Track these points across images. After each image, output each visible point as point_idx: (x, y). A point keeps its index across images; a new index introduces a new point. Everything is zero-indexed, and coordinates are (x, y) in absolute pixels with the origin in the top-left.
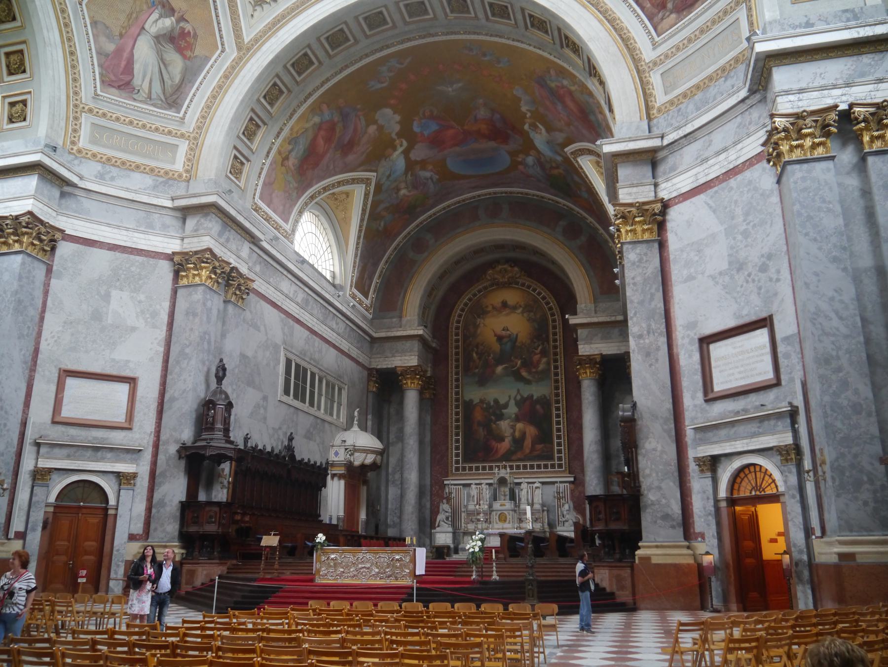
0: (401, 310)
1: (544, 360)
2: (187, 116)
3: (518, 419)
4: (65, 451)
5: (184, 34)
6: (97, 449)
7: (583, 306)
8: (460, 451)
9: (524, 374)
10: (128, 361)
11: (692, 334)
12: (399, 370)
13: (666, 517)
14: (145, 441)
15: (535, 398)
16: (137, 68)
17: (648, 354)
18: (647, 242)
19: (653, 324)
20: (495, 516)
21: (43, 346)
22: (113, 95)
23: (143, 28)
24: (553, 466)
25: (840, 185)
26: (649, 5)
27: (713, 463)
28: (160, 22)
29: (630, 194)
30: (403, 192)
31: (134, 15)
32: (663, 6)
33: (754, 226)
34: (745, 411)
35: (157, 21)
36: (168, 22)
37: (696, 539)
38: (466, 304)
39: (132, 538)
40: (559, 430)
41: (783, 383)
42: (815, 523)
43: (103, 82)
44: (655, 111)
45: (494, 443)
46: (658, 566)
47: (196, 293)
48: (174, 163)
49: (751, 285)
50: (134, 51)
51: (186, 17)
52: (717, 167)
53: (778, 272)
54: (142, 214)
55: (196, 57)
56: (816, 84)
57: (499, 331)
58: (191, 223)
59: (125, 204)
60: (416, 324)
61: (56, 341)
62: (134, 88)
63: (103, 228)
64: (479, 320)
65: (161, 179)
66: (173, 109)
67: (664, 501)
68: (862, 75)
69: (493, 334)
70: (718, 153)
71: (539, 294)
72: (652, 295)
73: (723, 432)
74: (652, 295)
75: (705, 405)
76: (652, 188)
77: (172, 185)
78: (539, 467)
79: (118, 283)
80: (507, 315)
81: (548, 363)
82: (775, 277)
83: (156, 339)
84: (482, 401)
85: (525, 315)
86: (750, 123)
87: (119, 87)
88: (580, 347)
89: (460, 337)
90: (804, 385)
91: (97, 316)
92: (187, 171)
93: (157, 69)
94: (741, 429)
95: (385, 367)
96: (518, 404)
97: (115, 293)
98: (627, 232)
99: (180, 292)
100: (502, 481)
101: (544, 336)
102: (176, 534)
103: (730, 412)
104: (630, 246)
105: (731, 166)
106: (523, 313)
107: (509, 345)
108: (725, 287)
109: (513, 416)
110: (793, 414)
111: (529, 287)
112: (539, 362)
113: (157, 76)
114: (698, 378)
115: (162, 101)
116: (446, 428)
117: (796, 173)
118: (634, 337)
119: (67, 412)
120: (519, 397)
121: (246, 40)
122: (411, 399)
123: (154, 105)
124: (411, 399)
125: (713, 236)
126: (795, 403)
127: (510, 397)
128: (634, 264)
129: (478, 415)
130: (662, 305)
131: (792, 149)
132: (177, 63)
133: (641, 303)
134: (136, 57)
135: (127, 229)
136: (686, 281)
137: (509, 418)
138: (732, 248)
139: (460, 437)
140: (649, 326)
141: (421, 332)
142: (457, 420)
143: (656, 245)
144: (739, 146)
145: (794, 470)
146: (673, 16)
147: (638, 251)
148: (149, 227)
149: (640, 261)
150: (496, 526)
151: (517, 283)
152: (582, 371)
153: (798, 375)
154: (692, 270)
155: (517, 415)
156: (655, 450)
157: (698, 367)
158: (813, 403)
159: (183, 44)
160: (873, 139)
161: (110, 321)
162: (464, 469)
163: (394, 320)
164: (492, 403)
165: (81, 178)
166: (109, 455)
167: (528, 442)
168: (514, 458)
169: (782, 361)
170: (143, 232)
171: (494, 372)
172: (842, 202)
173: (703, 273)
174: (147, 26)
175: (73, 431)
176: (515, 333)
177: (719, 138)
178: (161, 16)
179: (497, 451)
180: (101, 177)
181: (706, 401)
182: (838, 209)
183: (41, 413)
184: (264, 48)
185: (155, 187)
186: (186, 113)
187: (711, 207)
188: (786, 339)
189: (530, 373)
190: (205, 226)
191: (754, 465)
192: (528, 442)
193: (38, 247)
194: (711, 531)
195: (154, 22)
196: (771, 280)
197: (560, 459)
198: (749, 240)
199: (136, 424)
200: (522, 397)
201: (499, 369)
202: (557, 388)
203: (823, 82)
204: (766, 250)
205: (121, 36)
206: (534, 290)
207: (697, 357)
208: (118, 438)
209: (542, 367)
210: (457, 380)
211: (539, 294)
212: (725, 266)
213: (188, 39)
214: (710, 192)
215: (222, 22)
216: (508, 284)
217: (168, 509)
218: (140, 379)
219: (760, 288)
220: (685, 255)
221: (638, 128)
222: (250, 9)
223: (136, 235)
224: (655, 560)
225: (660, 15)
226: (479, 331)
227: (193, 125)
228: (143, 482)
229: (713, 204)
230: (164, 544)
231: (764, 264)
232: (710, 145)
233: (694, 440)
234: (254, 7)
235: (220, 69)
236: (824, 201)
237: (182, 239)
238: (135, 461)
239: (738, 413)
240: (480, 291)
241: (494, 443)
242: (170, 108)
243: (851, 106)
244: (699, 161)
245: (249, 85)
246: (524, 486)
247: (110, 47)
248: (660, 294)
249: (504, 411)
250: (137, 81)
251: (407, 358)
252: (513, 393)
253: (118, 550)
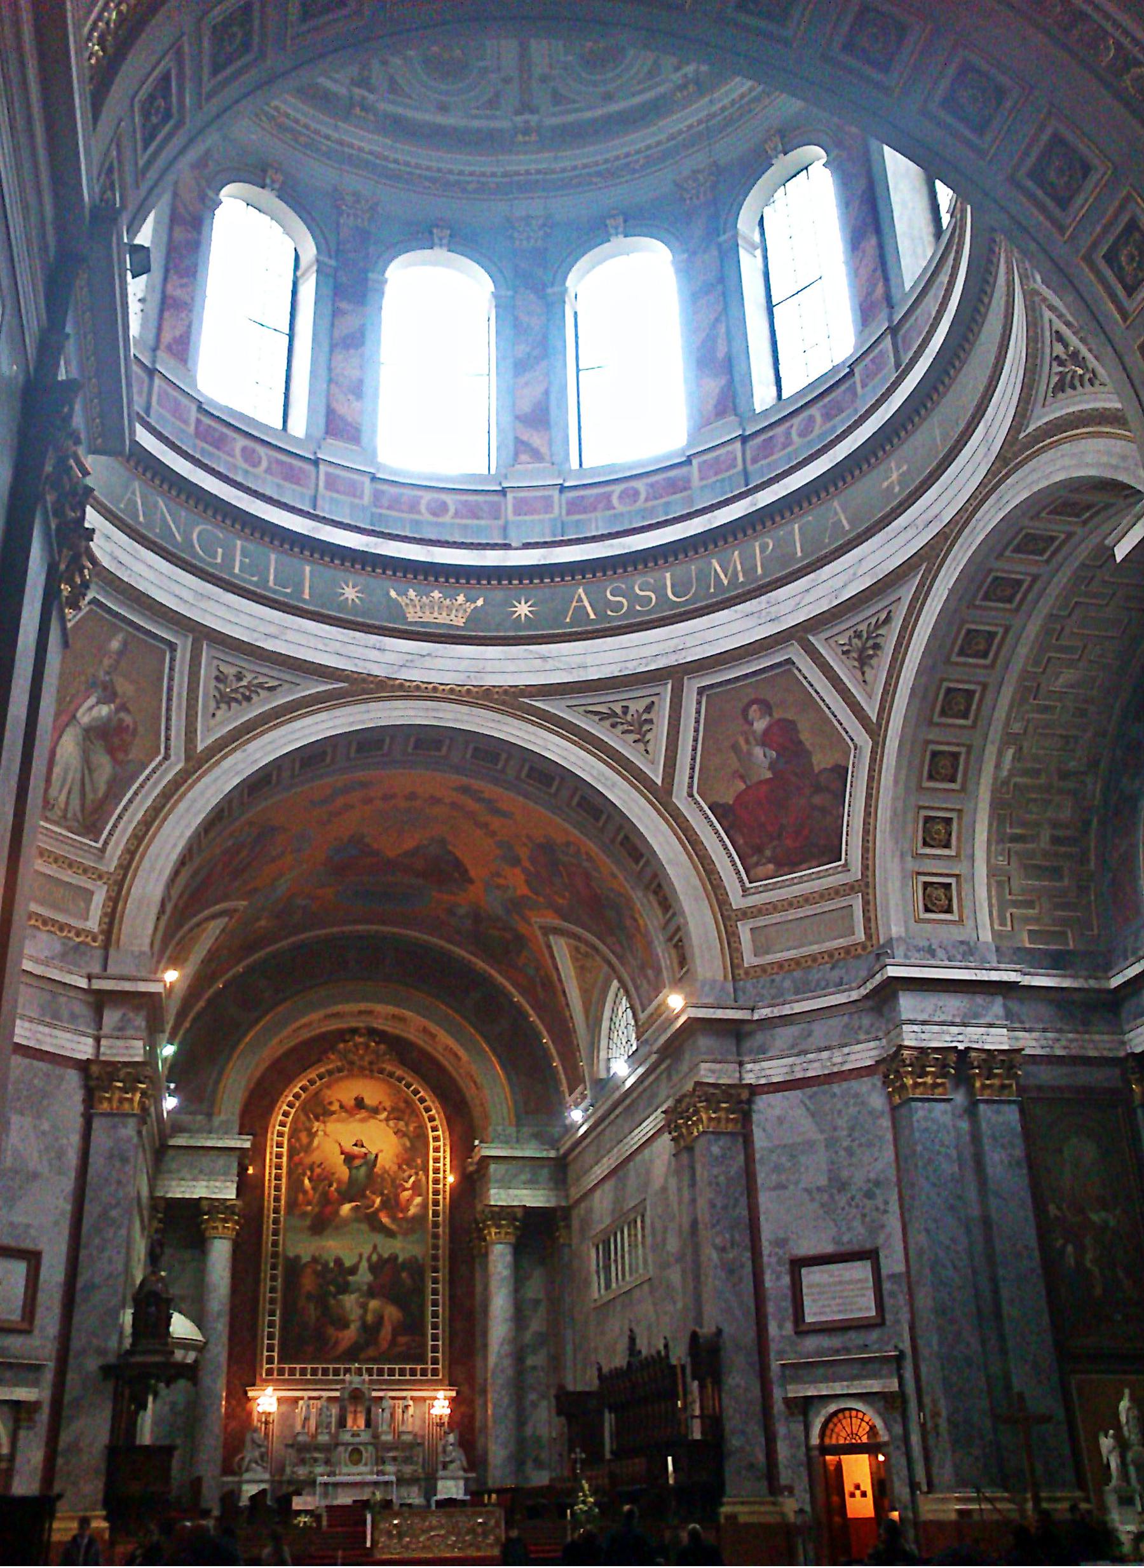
0: (212, 1104)
1: (418, 1200)
2: (109, 848)
3: (371, 1293)
5: (121, 729)
7: (500, 1128)
8: (276, 1342)
9: (385, 1220)
11: (781, 1252)
12: (205, 1205)
13: (751, 1466)
15: (400, 1260)
17: (731, 1272)
18: (731, 1134)
19: (737, 1237)
20: (342, 1453)
23: (74, 717)
24: (424, 1372)
25: (954, 1126)
26: (741, 842)
27: (804, 1407)
29: (713, 1071)
30: (263, 923)
32: (759, 850)
33: (860, 1145)
34: (847, 1350)
35: (91, 708)
36: (104, 710)
37: (781, 1494)
38: (297, 1096)
40: (435, 1315)
41: (888, 1323)
42: (920, 1475)
44: (741, 972)
45: (331, 1331)
46: (746, 1525)
47: (125, 1126)
48: (87, 919)
49: (854, 1210)
51: (129, 706)
52: (816, 1065)
53: (886, 1203)
55: (129, 762)
56: (936, 1019)
57: (348, 1146)
58: (111, 1018)
60: (236, 1130)
64: (316, 1124)
67: (748, 1448)
68: (976, 1016)
69: (337, 1150)
70: (820, 1050)
71: (416, 1092)
72: (737, 1200)
73: (821, 1371)
74: (737, 1200)
75: (795, 1338)
76: (736, 1066)
77: (84, 954)
78: (402, 1372)
80: (363, 1120)
81: (424, 1206)
82: (882, 1207)
84: (315, 1260)
85: (391, 1123)
86: (860, 1028)
88: (492, 1191)
89: (284, 1150)
90: (912, 1328)
93: (78, 776)
94: (841, 1370)
95: (179, 1196)
96: (373, 1268)
98: (710, 1119)
99: (96, 1124)
100: (356, 1396)
101: (419, 1161)
102: (100, 1496)
103: (829, 1349)
104: (712, 1137)
105: (835, 1070)
106: (387, 1120)
107: (363, 1170)
108: (822, 1205)
109: (365, 1288)
110: (900, 1358)
111: (400, 1080)
112: (409, 1201)
114: (787, 1304)
116: (256, 1300)
117: (920, 1111)
118: (715, 1247)
120: (375, 1258)
121: (200, 748)
122: (220, 1252)
124: (220, 1252)
125: (810, 1144)
126: (901, 1346)
127: (361, 1256)
128: (717, 1158)
129: (308, 1283)
130: (745, 1213)
131: (916, 1085)
133: (725, 1208)
136: (775, 1188)
137: (359, 1290)
138: (833, 1163)
139: (277, 1318)
140: (732, 1236)
141: (248, 1145)
142: (273, 1290)
143: (741, 1140)
144: (846, 1050)
145: (899, 1419)
146: (771, 866)
147: (721, 1143)
149: (723, 1156)
150: (345, 1470)
151: (381, 1071)
152: (493, 1230)
153: (905, 1316)
154: (783, 1177)
155: (371, 1287)
156: (738, 1386)
157: (789, 1292)
158: (924, 1352)
159: (116, 741)
160: (984, 1087)
162: (281, 1372)
163: (199, 1118)
164: (332, 1265)
167: (386, 1332)
168: (362, 1356)
169: (886, 1298)
170: (49, 1025)
171: (337, 1212)
172: (957, 1147)
173: (796, 1184)
174: (79, 715)
176: (374, 1152)
177: (820, 1031)
178: (98, 703)
179: (336, 1343)
181: (797, 1333)
182: (954, 1153)
184: (226, 764)
185: (63, 956)
186: (106, 843)
187: (808, 1109)
188: (892, 1276)
189: (394, 1218)
190: (137, 1023)
191: (850, 1409)
192: (386, 1332)
194: (802, 1486)
196: (877, 1209)
197: (435, 1361)
198: (854, 1160)
200: (380, 1256)
201: (346, 1209)
202: (435, 1247)
203: (943, 1018)
204: (872, 1176)
206: (408, 1086)
207: (786, 1280)
209: (412, 1211)
210: (276, 1222)
211: (416, 1092)
212: (823, 1181)
214: (809, 1091)
215: (174, 718)
216: (371, 1071)
217: (85, 1457)
219: (864, 1216)
220: (774, 1157)
221: (723, 989)
222: (213, 704)
224: (742, 1519)
225: (755, 859)
226: (316, 1143)
227: (115, 863)
228: (44, 1416)
229: (812, 1107)
231: (869, 1190)
232: (809, 1035)
233: (783, 1376)
234: (218, 703)
235: (155, 784)
236: (942, 1144)
238: (35, 1384)
239: (837, 1352)
240: (321, 1077)
241: (331, 1331)
243: (968, 1049)
244: (796, 1051)
245: (203, 816)
246: (385, 1404)
248: (743, 1201)
249: (350, 1278)
251: (218, 1184)
252: (367, 1250)
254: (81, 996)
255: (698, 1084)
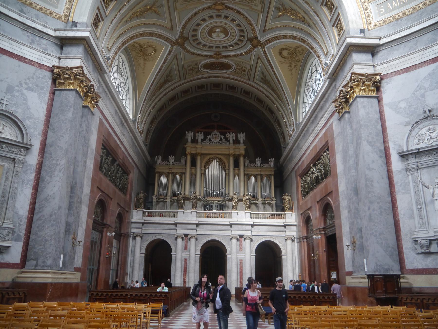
92: (66, 16)
237: (60, 59)
254: (52, 40)
255: (352, 74)
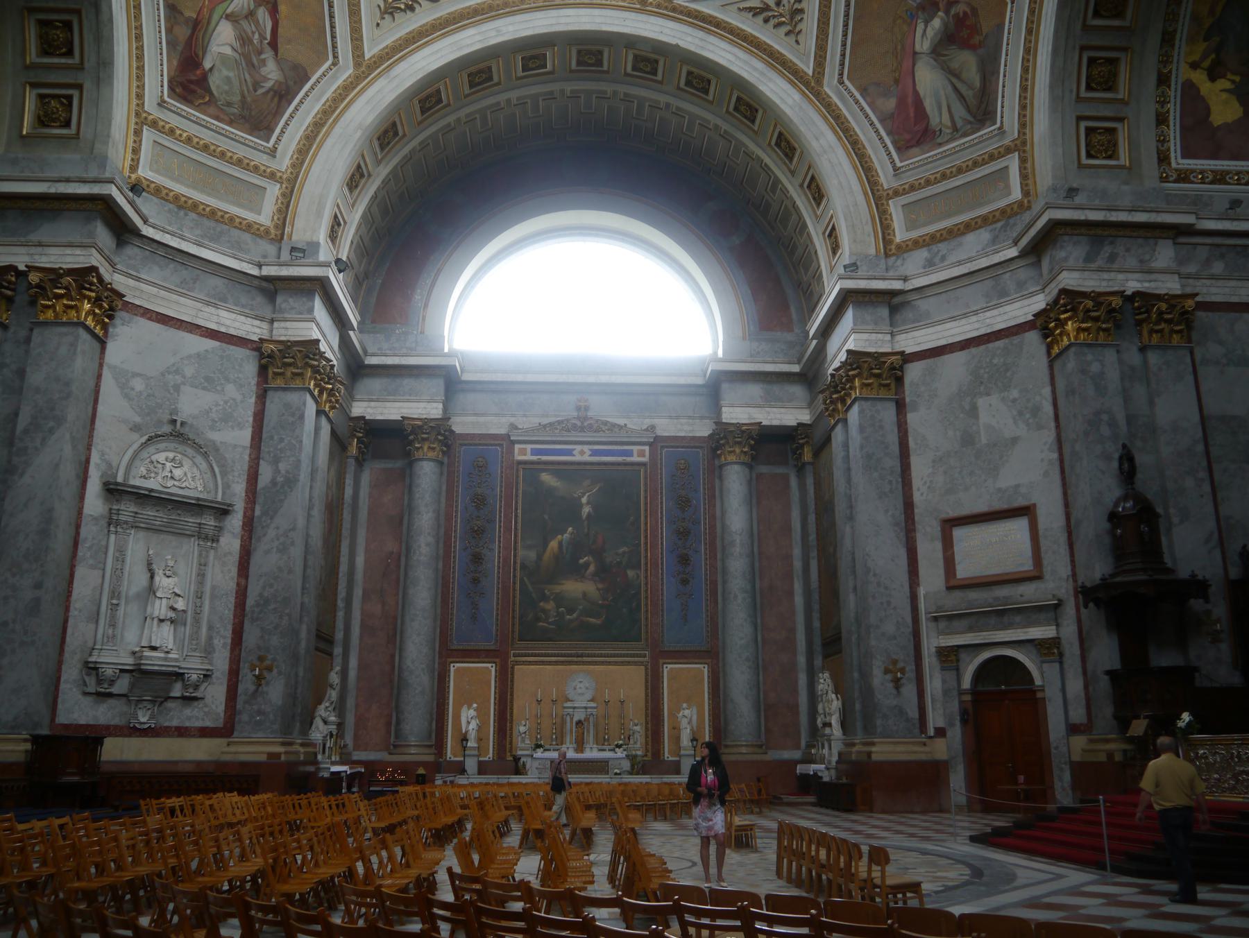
4: (964, 623)
6: (1001, 613)
10: (1018, 486)
14: (1063, 591)
16: (929, 105)
21: (917, 497)
22: (918, 157)
23: (915, 53)
28: (929, 29)
31: (899, 47)
35: (925, 31)
36: (936, 23)
39: (1073, 729)
43: (899, 150)
50: (918, 88)
54: (989, 283)
59: (966, 281)
61: (929, 487)
62: (934, 132)
63: (948, 325)
65: (999, 225)
66: (988, 123)
79: (982, 388)
83: (1045, 444)
87: (919, 143)
91: (968, 439)
93: (950, 88)
97: (981, 402)
113: (953, 96)
115: (970, 123)
119: (964, 571)
123: (965, 135)
132: (967, 61)
134: (922, 94)
135: (976, 313)
148: (1001, 296)
161: (984, 441)
165: (905, 279)
166: (1018, 619)
174: (918, 48)
175: (974, 595)
180: (930, 264)
183: (932, 579)
185: (994, 241)
193: (875, 385)
195: (923, 37)
199: (1047, 570)
205: (897, 81)
208: (1028, 592)
213: (968, 23)
218: (1038, 506)
223: (988, 314)
230: (1103, 737)
242: (984, 125)
247: (891, 104)
250: (934, 121)
253: (1056, 748)
254: (1022, 263)
